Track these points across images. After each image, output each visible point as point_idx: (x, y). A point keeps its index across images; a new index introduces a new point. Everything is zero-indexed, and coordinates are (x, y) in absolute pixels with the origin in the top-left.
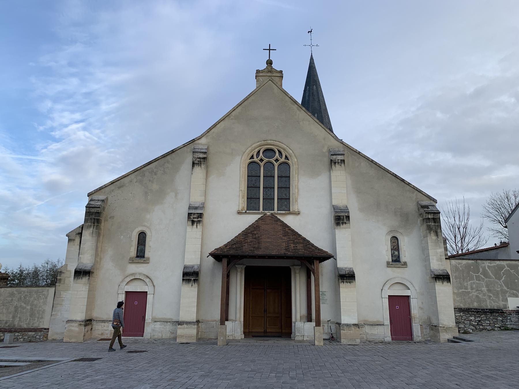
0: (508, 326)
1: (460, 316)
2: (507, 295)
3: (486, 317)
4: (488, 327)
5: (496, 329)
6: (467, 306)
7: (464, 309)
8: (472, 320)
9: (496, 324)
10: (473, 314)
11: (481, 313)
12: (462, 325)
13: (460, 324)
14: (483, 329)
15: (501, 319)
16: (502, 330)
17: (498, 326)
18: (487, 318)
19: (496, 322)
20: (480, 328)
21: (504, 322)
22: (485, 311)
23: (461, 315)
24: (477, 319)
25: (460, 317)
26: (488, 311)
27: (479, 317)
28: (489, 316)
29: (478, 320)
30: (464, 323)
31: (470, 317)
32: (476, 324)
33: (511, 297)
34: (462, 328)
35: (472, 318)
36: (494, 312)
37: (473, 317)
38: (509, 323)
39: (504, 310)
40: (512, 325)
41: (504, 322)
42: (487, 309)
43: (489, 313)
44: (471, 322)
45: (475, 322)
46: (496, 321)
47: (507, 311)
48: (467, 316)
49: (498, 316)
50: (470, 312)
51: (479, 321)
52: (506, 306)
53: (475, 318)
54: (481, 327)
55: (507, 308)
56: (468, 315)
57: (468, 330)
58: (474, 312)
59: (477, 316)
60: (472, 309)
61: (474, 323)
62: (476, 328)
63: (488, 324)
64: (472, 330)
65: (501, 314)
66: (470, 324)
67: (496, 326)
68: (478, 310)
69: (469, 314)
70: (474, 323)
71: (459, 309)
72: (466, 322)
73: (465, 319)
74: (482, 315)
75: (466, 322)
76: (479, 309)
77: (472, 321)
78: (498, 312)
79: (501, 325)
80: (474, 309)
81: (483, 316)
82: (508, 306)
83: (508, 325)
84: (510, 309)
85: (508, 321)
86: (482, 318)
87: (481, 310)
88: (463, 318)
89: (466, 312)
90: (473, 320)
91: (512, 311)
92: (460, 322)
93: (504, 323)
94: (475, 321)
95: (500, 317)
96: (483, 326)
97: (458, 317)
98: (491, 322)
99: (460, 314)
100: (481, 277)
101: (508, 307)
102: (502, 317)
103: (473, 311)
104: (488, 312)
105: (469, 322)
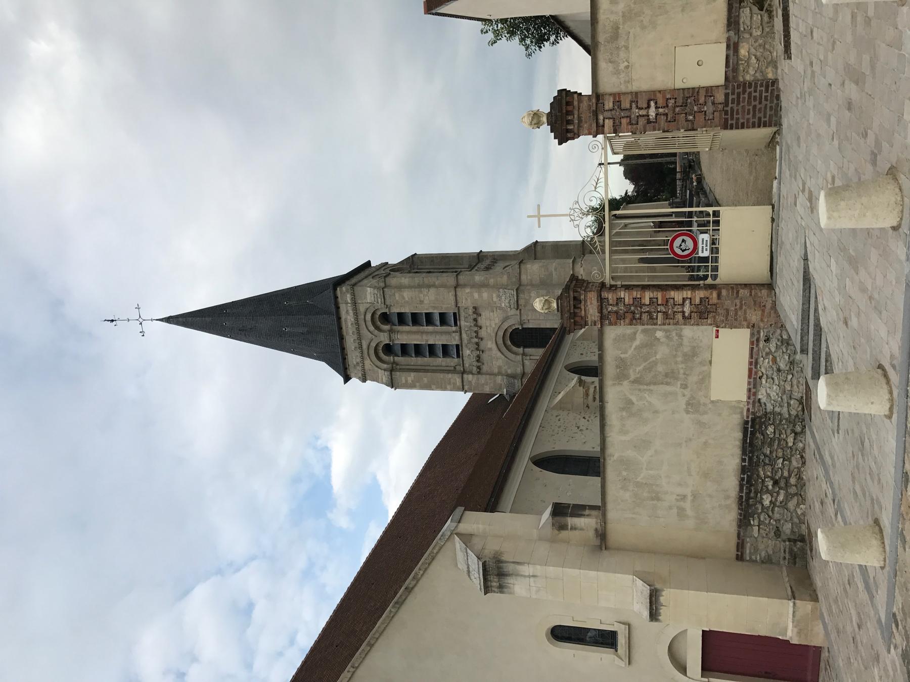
0: (792, 413)
1: (759, 526)
2: (703, 400)
3: (765, 464)
4: (795, 463)
5: (801, 445)
6: (732, 503)
7: (740, 514)
8: (771, 502)
9: (787, 443)
10: (756, 493)
11: (752, 474)
12: (784, 528)
13: (781, 529)
14: (800, 478)
15: (770, 430)
16: (803, 432)
17: (792, 440)
18: (767, 461)
19: (779, 441)
20: (796, 486)
21: (781, 421)
22: (749, 465)
23: (756, 523)
24: (770, 487)
25: (761, 526)
26: (747, 459)
27: (763, 481)
28: (762, 457)
29: (773, 486)
30: (778, 521)
31: (765, 503)
32: (785, 494)
33: (708, 388)
34: (792, 528)
35: (767, 500)
36: (751, 444)
37: (764, 497)
38: (785, 410)
39: (748, 417)
40: (792, 402)
41: (781, 421)
42: (743, 460)
43: (753, 456)
44: (778, 504)
45: (778, 493)
46: (777, 442)
47: (748, 410)
48: (760, 511)
49: (763, 435)
50: (751, 503)
51: (776, 483)
52: (733, 407)
53: (768, 491)
54: (793, 481)
55: (742, 406)
56: (757, 509)
57: (799, 513)
58: (750, 491)
59: (760, 486)
60: (741, 497)
61: (781, 498)
62: (796, 494)
63: (785, 462)
64: (802, 506)
65: (757, 427)
66: (784, 505)
67: (790, 444)
68: (745, 483)
69: (756, 504)
70: (781, 498)
71: (739, 526)
72: (777, 516)
73: (769, 516)
74: (758, 476)
75: (777, 516)
76: (743, 479)
77: (776, 499)
78: (753, 433)
79: (789, 431)
80: (741, 490)
81: (762, 473)
82: (734, 404)
83: (789, 414)
84: (745, 398)
85: (777, 409)
86: (769, 477)
87: (746, 476)
88: (767, 522)
89: (750, 511)
90: (773, 499)
91: (749, 398)
92: (777, 527)
93: (784, 421)
94: (775, 494)
95: (766, 428)
96: (790, 476)
97: (761, 531)
98: (780, 454)
99: (755, 526)
100: (652, 456)
101: (739, 402)
102: (767, 424)
103: (748, 494)
104: (751, 459)
105: (776, 509)
